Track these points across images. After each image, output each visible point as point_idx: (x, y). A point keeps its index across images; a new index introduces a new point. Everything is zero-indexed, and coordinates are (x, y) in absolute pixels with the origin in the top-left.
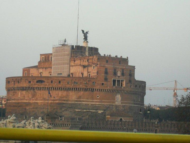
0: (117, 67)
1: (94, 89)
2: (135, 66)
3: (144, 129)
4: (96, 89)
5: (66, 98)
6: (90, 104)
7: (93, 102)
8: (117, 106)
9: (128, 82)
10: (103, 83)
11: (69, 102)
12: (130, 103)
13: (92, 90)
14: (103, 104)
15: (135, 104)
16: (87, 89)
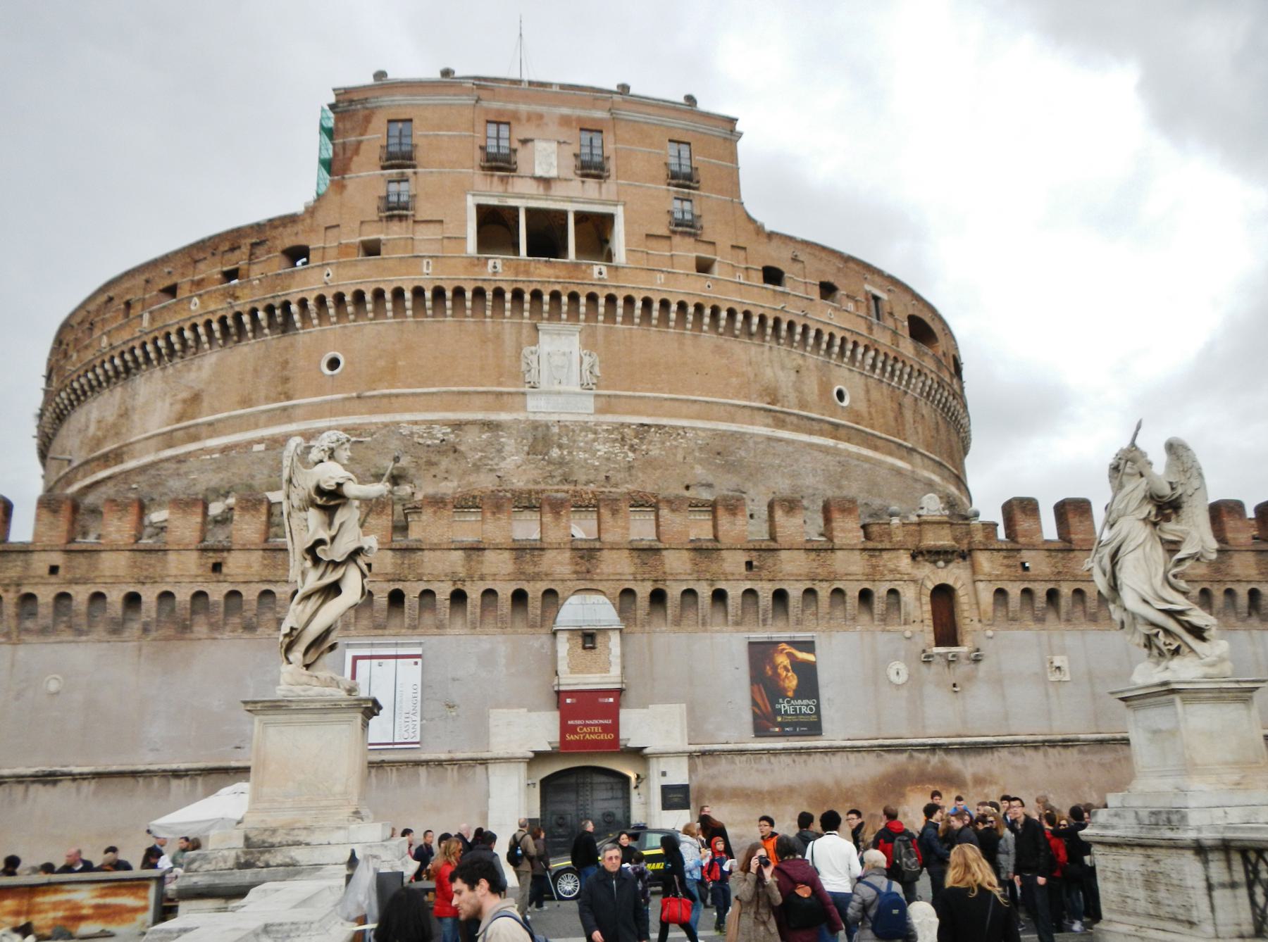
0: (523, 108)
1: (286, 306)
2: (732, 121)
3: (734, 592)
4: (303, 303)
5: (117, 434)
6: (260, 441)
7: (286, 415)
8: (540, 439)
9: (666, 233)
10: (378, 242)
11: (130, 464)
12: (707, 410)
13: (281, 318)
14: (386, 425)
15: (780, 420)
16: (238, 317)
